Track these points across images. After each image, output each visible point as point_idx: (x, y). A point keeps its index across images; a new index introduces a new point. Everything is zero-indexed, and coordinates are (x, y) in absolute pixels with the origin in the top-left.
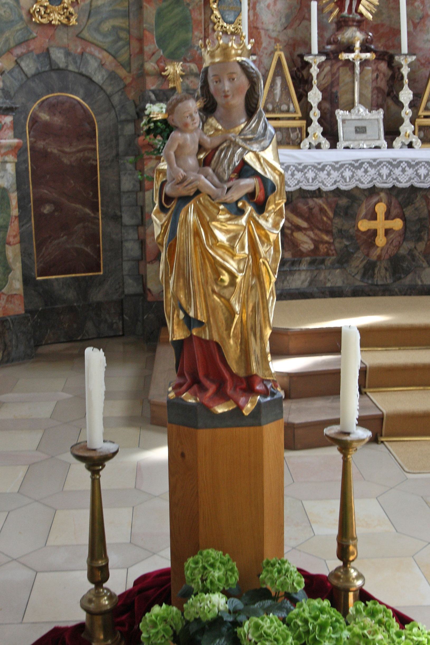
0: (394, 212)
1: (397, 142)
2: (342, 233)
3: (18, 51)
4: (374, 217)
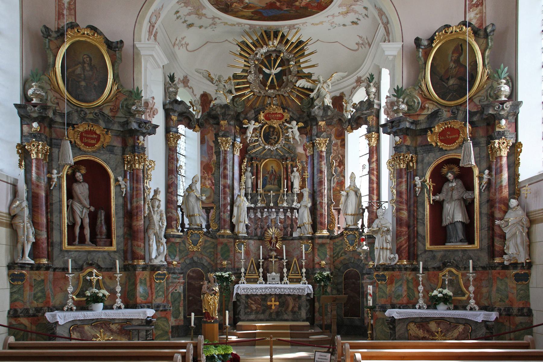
0: (277, 300)
2: (263, 305)
3: (185, 258)
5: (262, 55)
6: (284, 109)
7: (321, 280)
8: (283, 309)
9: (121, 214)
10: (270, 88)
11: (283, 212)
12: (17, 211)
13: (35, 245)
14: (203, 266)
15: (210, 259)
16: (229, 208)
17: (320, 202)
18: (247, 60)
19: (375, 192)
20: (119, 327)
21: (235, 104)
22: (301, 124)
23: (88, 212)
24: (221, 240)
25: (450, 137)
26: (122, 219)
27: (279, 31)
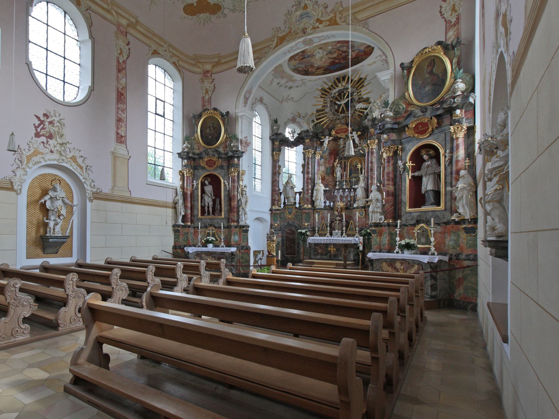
1: (343, 236)
4: (331, 248)
8: (339, 253)
9: (227, 200)
10: (341, 113)
11: (353, 191)
12: (176, 201)
14: (295, 227)
15: (299, 222)
16: (310, 191)
18: (325, 99)
21: (316, 128)
22: (359, 133)
23: (211, 199)
24: (305, 211)
25: (422, 129)
26: (227, 202)
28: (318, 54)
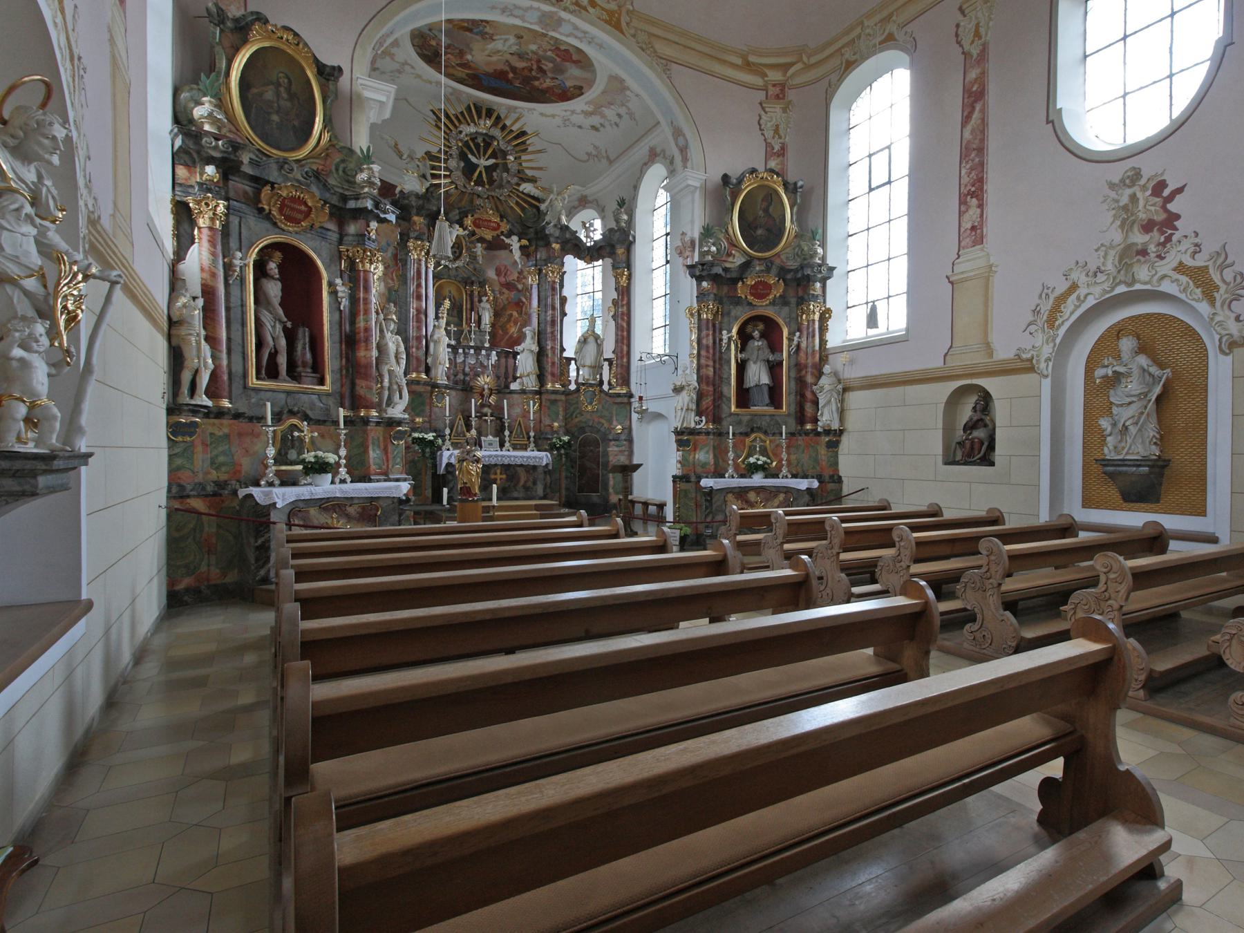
4: (496, 474)
5: (467, 135)
6: (502, 217)
7: (563, 446)
13: (214, 376)
17: (552, 348)
19: (625, 341)
20: (360, 510)
27: (494, 110)
28: (502, 41)
